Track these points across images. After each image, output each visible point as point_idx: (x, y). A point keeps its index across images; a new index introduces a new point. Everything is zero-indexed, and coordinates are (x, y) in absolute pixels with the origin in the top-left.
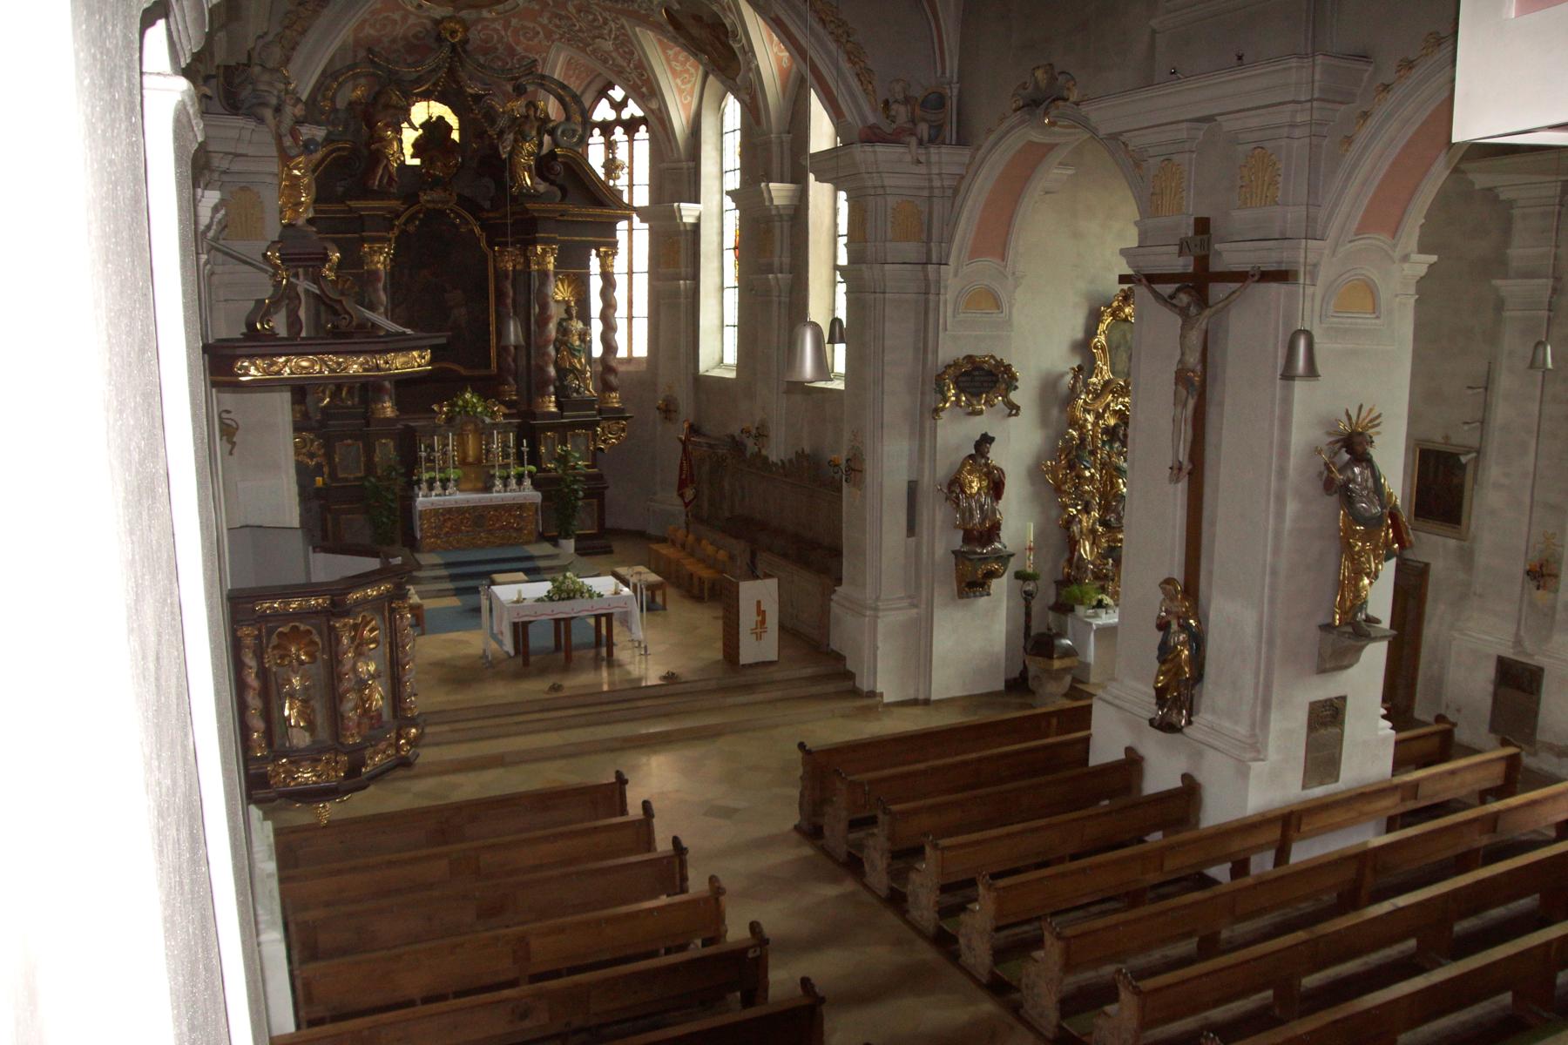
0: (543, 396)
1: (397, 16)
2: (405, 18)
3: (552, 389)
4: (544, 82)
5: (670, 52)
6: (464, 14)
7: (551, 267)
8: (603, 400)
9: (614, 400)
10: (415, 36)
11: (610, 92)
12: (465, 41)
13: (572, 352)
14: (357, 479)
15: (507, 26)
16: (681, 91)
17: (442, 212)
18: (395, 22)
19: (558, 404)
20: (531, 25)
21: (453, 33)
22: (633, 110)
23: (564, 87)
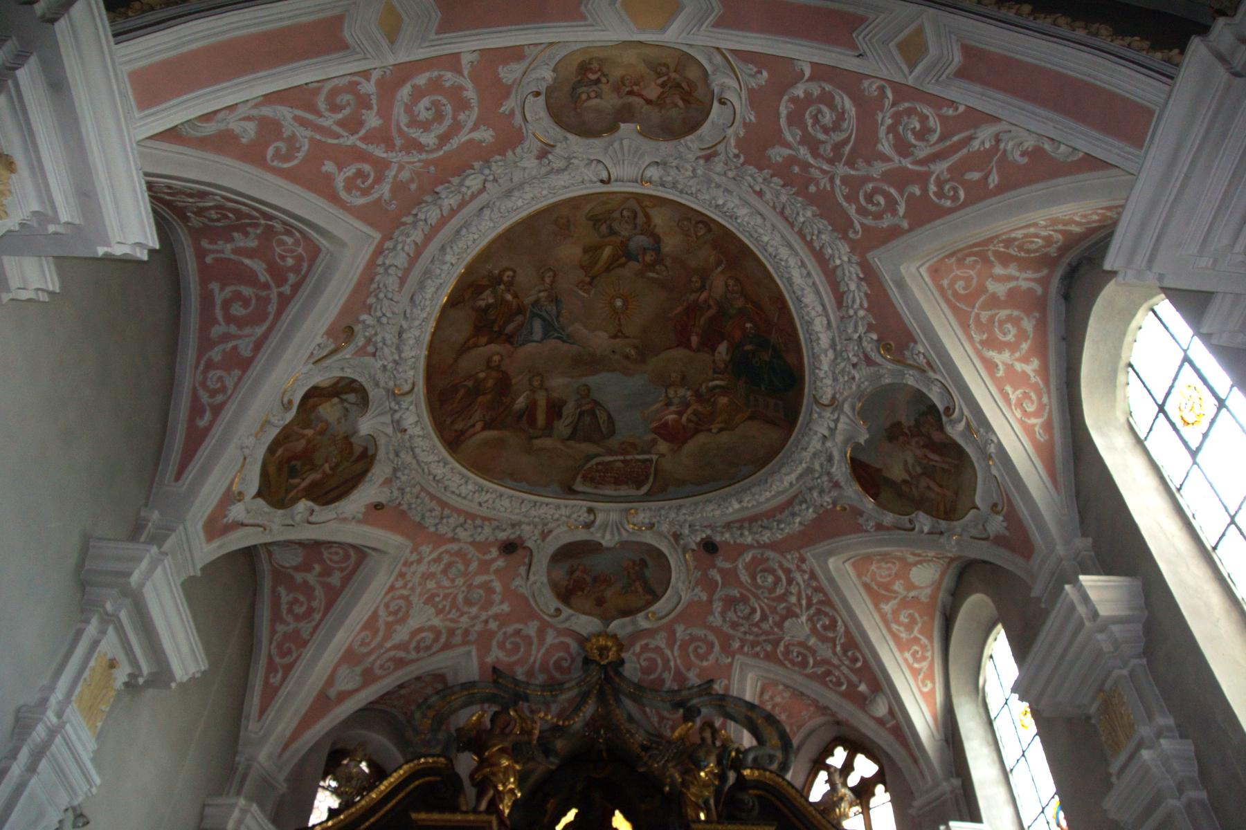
1: (532, 629)
2: (541, 633)
4: (724, 703)
5: (887, 608)
6: (614, 626)
10: (558, 665)
11: (830, 761)
15: (671, 639)
16: (915, 672)
18: (528, 639)
20: (700, 632)
21: (603, 650)
22: (865, 767)
23: (752, 706)
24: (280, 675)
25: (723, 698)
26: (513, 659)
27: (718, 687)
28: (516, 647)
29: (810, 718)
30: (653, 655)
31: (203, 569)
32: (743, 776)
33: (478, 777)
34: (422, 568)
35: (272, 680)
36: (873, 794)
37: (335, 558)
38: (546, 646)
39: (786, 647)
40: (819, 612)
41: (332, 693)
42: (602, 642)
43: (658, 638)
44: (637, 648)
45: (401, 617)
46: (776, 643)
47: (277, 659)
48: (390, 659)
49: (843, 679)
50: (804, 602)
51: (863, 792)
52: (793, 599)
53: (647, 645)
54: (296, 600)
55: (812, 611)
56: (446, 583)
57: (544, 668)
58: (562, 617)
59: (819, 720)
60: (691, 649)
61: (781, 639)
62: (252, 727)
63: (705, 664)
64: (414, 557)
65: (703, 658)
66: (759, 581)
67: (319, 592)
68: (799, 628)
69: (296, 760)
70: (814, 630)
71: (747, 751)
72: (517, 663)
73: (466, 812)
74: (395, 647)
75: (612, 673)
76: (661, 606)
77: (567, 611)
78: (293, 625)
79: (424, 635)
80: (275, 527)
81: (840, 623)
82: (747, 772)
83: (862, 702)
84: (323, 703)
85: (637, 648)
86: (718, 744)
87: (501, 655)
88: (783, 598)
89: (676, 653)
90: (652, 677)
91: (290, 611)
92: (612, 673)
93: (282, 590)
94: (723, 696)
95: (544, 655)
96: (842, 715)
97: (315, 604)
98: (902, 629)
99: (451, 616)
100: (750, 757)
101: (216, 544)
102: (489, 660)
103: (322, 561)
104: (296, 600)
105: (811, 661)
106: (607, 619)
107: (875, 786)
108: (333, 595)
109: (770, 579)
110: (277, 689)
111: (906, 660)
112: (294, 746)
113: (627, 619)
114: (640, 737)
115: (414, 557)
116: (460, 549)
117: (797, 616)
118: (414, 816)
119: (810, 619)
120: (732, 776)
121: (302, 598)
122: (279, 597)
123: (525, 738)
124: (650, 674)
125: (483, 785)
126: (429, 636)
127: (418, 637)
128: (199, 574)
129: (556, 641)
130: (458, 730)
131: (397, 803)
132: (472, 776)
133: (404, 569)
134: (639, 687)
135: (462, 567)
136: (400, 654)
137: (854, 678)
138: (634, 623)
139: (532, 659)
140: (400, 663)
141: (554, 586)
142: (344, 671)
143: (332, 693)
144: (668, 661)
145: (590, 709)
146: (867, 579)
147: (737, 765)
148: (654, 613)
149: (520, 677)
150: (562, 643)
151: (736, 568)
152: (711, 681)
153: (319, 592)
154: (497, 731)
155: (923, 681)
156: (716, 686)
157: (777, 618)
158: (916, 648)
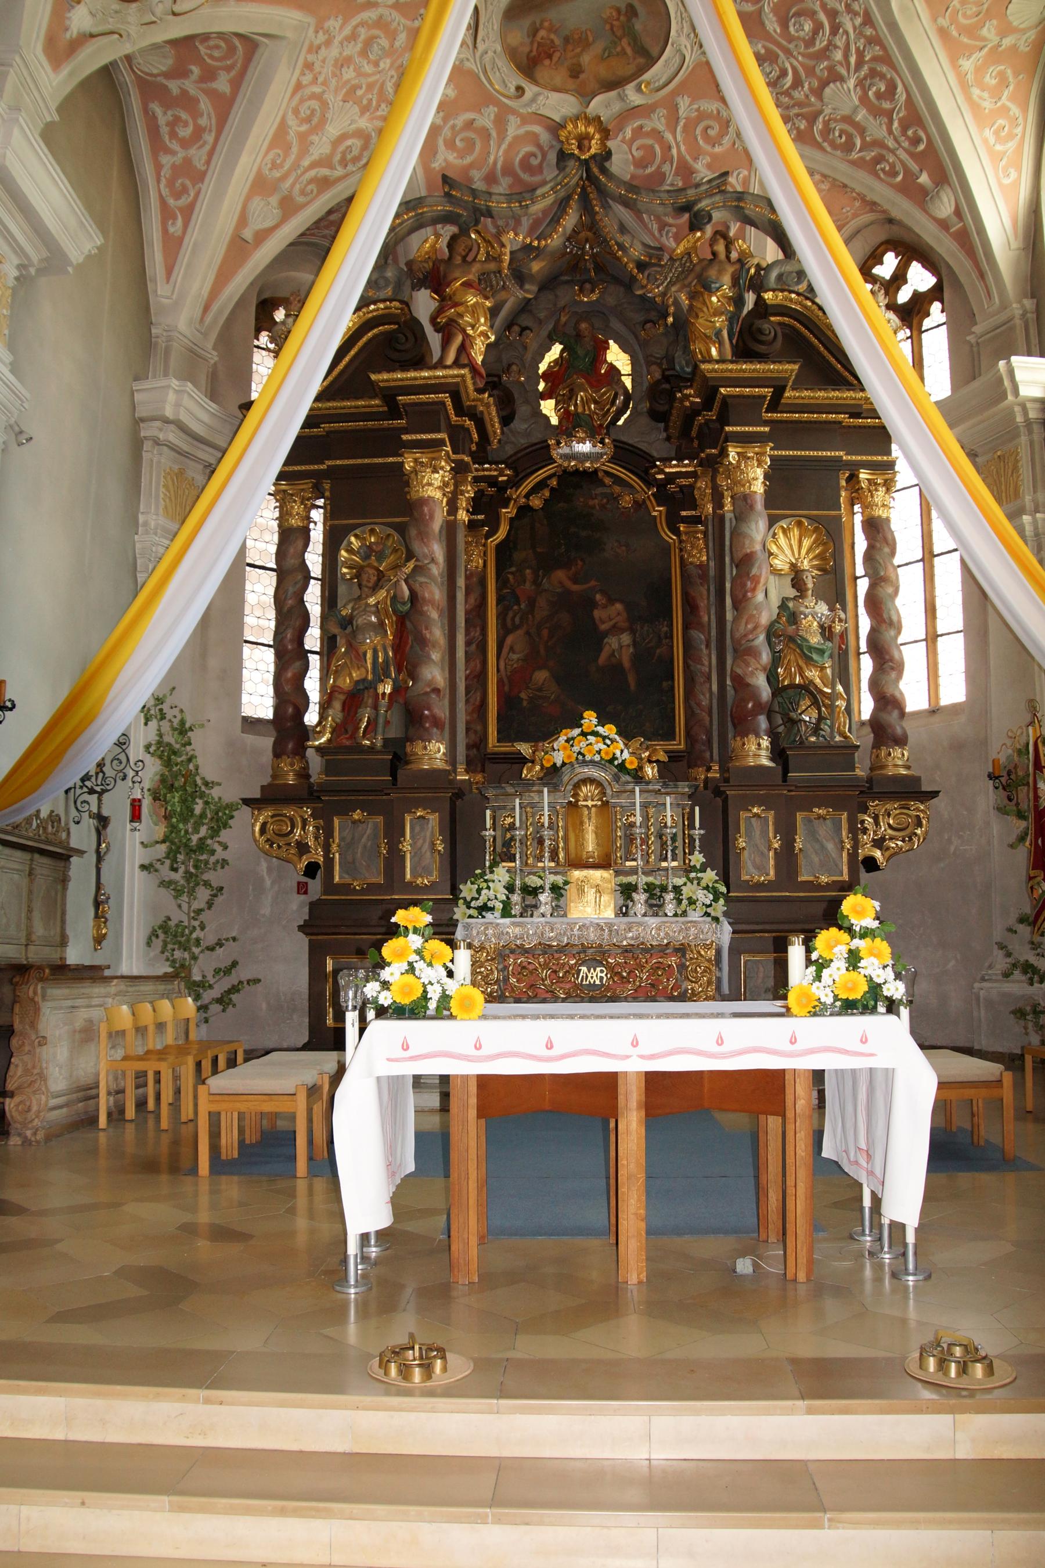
0: (744, 734)
1: (486, 119)
2: (500, 122)
3: (763, 722)
7: (759, 487)
8: (876, 766)
9: (898, 761)
10: (525, 164)
11: (877, 270)
12: (607, 155)
13: (807, 655)
14: (371, 888)
15: (673, 119)
16: (996, 157)
17: (592, 477)
18: (485, 133)
19: (778, 753)
21: (583, 140)
22: (920, 279)
24: (180, 222)
25: (740, 196)
26: (468, 160)
27: (735, 182)
28: (470, 145)
29: (855, 216)
30: (649, 142)
31: (60, 109)
32: (764, 300)
33: (442, 320)
34: (334, 52)
35: (171, 230)
36: (928, 315)
37: (216, 54)
38: (509, 139)
39: (826, 123)
40: (873, 73)
41: (248, 234)
42: (582, 128)
43: (654, 116)
44: (628, 133)
45: (316, 123)
46: (812, 119)
47: (171, 202)
48: (311, 181)
49: (899, 167)
50: (853, 60)
51: (911, 314)
52: (838, 56)
53: (641, 127)
54: (177, 119)
55: (865, 71)
56: (368, 69)
57: (508, 170)
58: (529, 94)
59: (867, 218)
60: (698, 131)
61: (820, 112)
62: (161, 291)
63: (717, 149)
64: (321, 38)
65: (713, 142)
66: (792, 29)
67: (205, 104)
68: (844, 97)
69: (221, 321)
70: (864, 99)
71: (769, 267)
72: (471, 166)
73: (435, 367)
74: (314, 165)
75: (595, 170)
76: (657, 72)
77: (530, 90)
78: (181, 154)
79: (349, 142)
80: (133, 30)
81: (900, 88)
82: (768, 296)
83: (922, 197)
84: (240, 247)
85: (628, 133)
86: (734, 255)
87: (452, 157)
88: (824, 54)
89: (679, 138)
90: (649, 171)
91: (173, 135)
92: (595, 170)
93: (156, 108)
94: (742, 193)
95: (506, 152)
96: (895, 214)
97: (203, 122)
98: (985, 95)
99: (379, 113)
100: (774, 275)
101: (65, 70)
102: (437, 165)
103: (200, 61)
104: (177, 119)
105: (858, 142)
106: (586, 95)
107: (931, 303)
108: (224, 106)
109: (808, 26)
110: (181, 239)
111: (985, 141)
112: (215, 308)
113: (613, 94)
114: (636, 252)
115: (321, 38)
116: (381, 17)
117: (842, 79)
118: (373, 377)
119: (860, 83)
120: (750, 298)
121: (184, 116)
122: (154, 118)
123: (492, 266)
124: (646, 167)
125: (447, 330)
126: (356, 143)
127: (342, 148)
128: (57, 118)
129: (521, 131)
130: (409, 264)
131: (351, 361)
132: (433, 320)
133: (311, 58)
134: (631, 187)
135: (384, 42)
136: (325, 172)
137: (914, 166)
138: (622, 98)
139: (492, 158)
140: (325, 183)
141: (512, 54)
142: (257, 203)
143: (248, 234)
144: (670, 148)
145: (570, 220)
146: (943, 22)
147: (758, 284)
148: (648, 84)
149: (479, 185)
150: (528, 133)
151: (760, 10)
152: (726, 174)
153: (205, 104)
154: (458, 260)
155: (1005, 170)
156: (732, 180)
157: (816, 84)
158: (1001, 122)
